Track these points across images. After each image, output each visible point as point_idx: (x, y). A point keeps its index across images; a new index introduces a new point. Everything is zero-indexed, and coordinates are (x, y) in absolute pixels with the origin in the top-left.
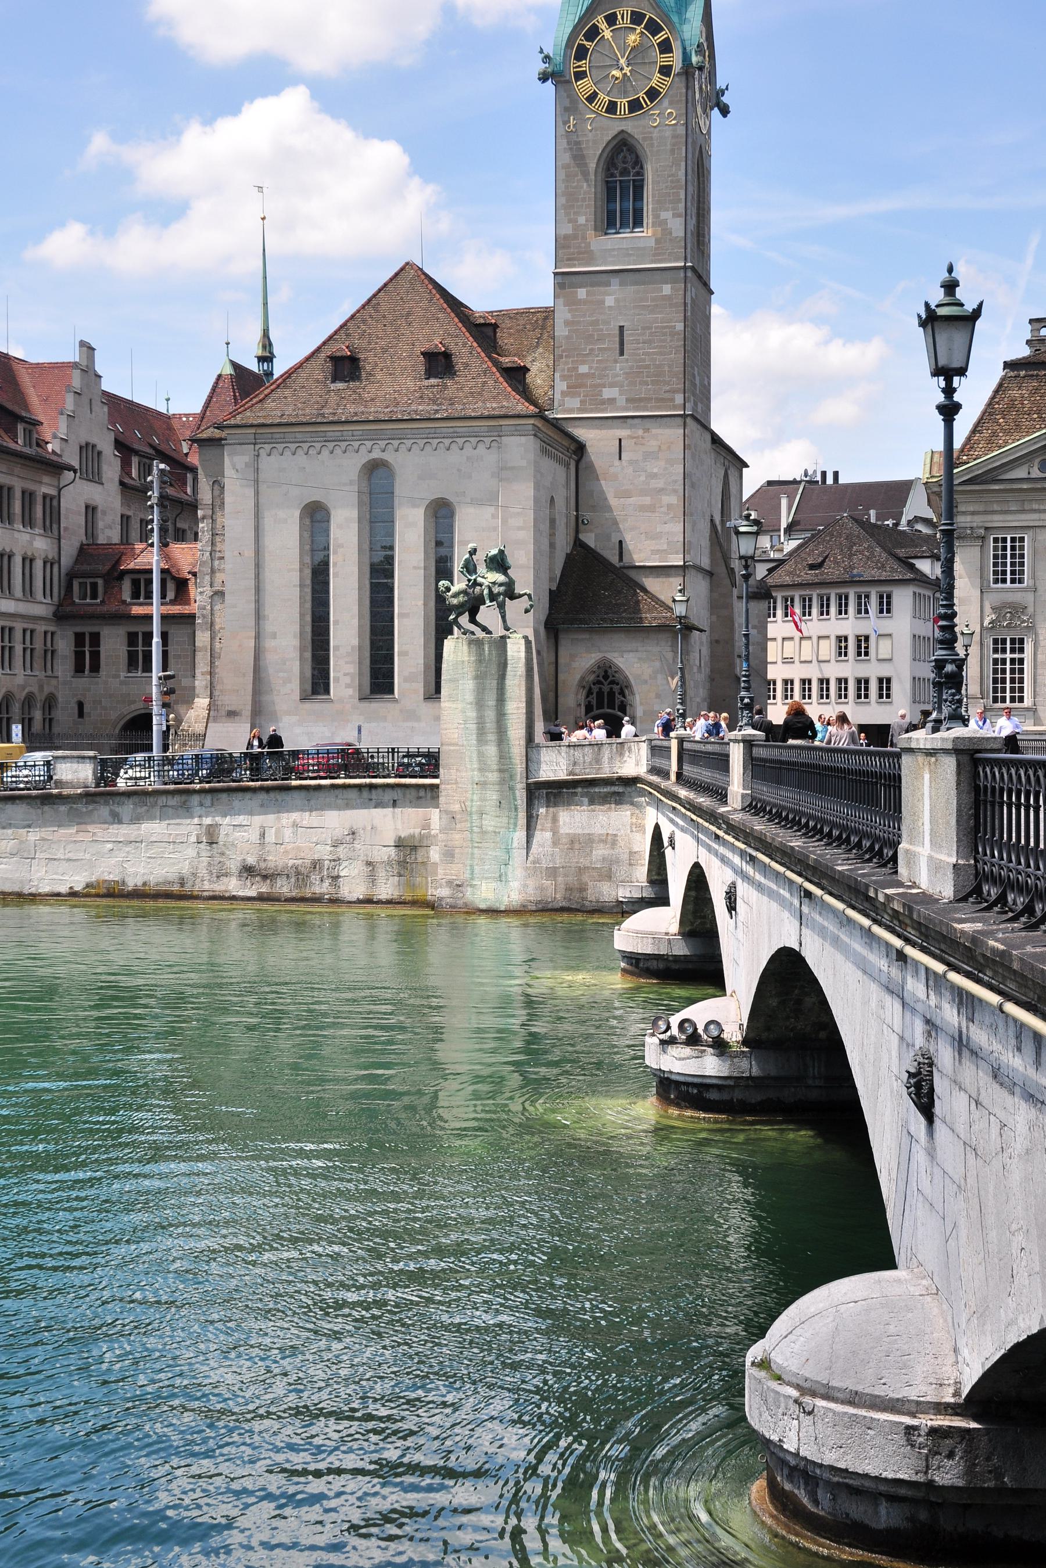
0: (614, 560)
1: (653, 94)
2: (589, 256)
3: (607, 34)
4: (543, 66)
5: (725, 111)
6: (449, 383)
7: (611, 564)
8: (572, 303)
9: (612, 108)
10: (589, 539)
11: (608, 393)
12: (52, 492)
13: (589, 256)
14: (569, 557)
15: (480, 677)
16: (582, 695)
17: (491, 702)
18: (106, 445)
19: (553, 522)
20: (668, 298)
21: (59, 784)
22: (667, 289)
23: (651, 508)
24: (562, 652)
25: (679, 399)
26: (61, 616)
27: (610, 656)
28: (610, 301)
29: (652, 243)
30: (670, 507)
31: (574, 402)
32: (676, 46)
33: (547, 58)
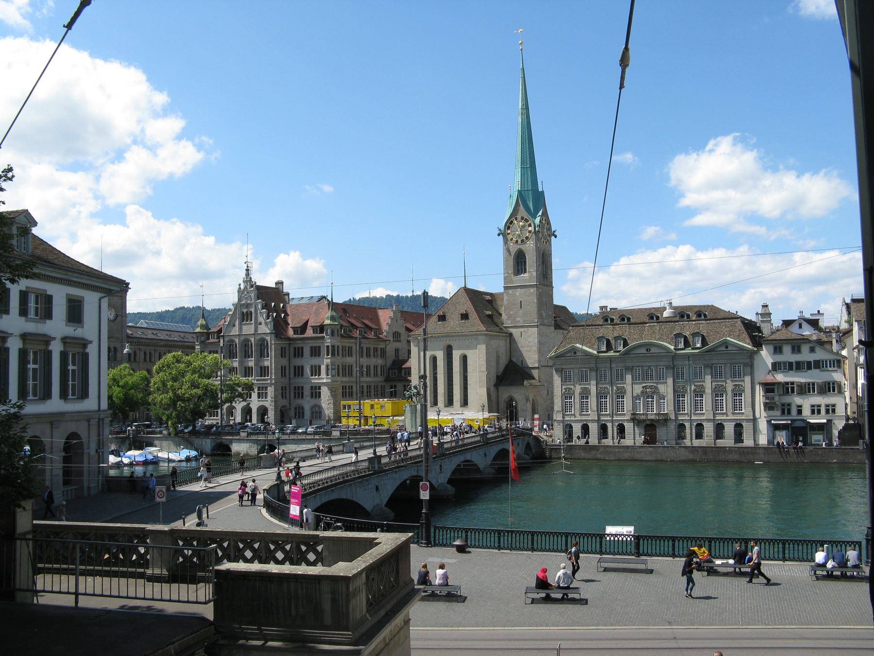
0: (520, 365)
1: (527, 238)
2: (512, 282)
3: (516, 222)
4: (498, 232)
5: (556, 237)
6: (466, 321)
7: (519, 366)
8: (508, 294)
9: (517, 242)
10: (514, 360)
11: (518, 319)
12: (384, 347)
13: (512, 282)
14: (507, 367)
15: (412, 413)
16: (505, 404)
17: (414, 419)
18: (402, 331)
19: (498, 357)
20: (533, 292)
21: (334, 436)
22: (532, 290)
23: (529, 351)
24: (499, 393)
25: (536, 320)
26: (386, 381)
27: (512, 394)
28: (518, 294)
29: (528, 278)
30: (534, 350)
31: (509, 322)
32: (533, 225)
33: (500, 229)
